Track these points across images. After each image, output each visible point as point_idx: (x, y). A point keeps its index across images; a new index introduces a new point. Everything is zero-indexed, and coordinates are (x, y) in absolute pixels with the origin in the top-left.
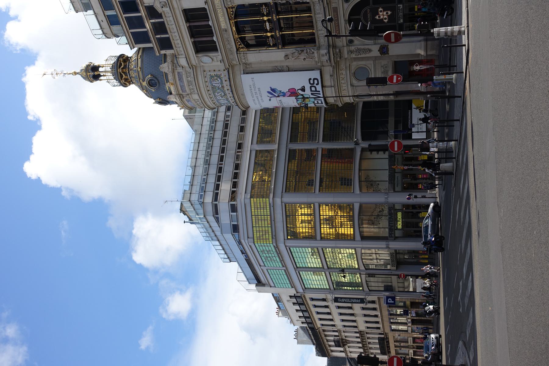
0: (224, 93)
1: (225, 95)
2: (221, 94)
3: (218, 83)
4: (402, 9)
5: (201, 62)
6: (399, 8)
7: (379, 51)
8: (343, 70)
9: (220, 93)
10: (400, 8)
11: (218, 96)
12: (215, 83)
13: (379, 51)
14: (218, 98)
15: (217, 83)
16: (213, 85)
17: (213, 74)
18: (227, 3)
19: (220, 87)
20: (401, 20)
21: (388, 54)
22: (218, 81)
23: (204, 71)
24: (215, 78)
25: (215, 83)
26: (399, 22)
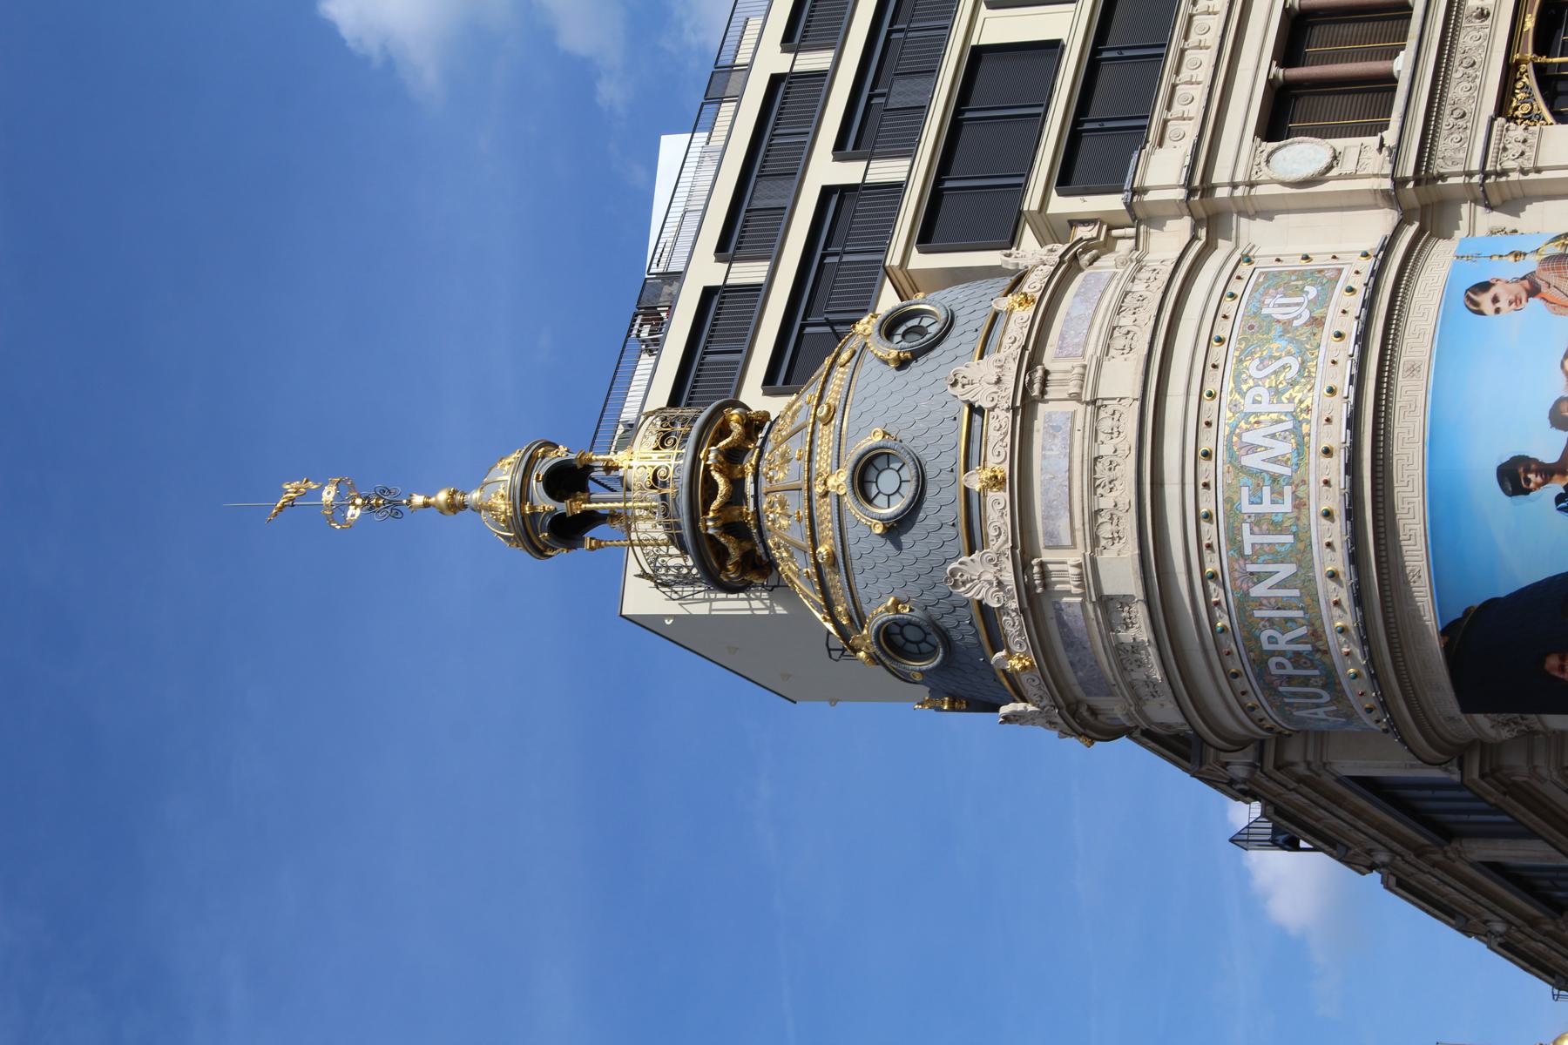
9: (1276, 365)
19: (1296, 323)
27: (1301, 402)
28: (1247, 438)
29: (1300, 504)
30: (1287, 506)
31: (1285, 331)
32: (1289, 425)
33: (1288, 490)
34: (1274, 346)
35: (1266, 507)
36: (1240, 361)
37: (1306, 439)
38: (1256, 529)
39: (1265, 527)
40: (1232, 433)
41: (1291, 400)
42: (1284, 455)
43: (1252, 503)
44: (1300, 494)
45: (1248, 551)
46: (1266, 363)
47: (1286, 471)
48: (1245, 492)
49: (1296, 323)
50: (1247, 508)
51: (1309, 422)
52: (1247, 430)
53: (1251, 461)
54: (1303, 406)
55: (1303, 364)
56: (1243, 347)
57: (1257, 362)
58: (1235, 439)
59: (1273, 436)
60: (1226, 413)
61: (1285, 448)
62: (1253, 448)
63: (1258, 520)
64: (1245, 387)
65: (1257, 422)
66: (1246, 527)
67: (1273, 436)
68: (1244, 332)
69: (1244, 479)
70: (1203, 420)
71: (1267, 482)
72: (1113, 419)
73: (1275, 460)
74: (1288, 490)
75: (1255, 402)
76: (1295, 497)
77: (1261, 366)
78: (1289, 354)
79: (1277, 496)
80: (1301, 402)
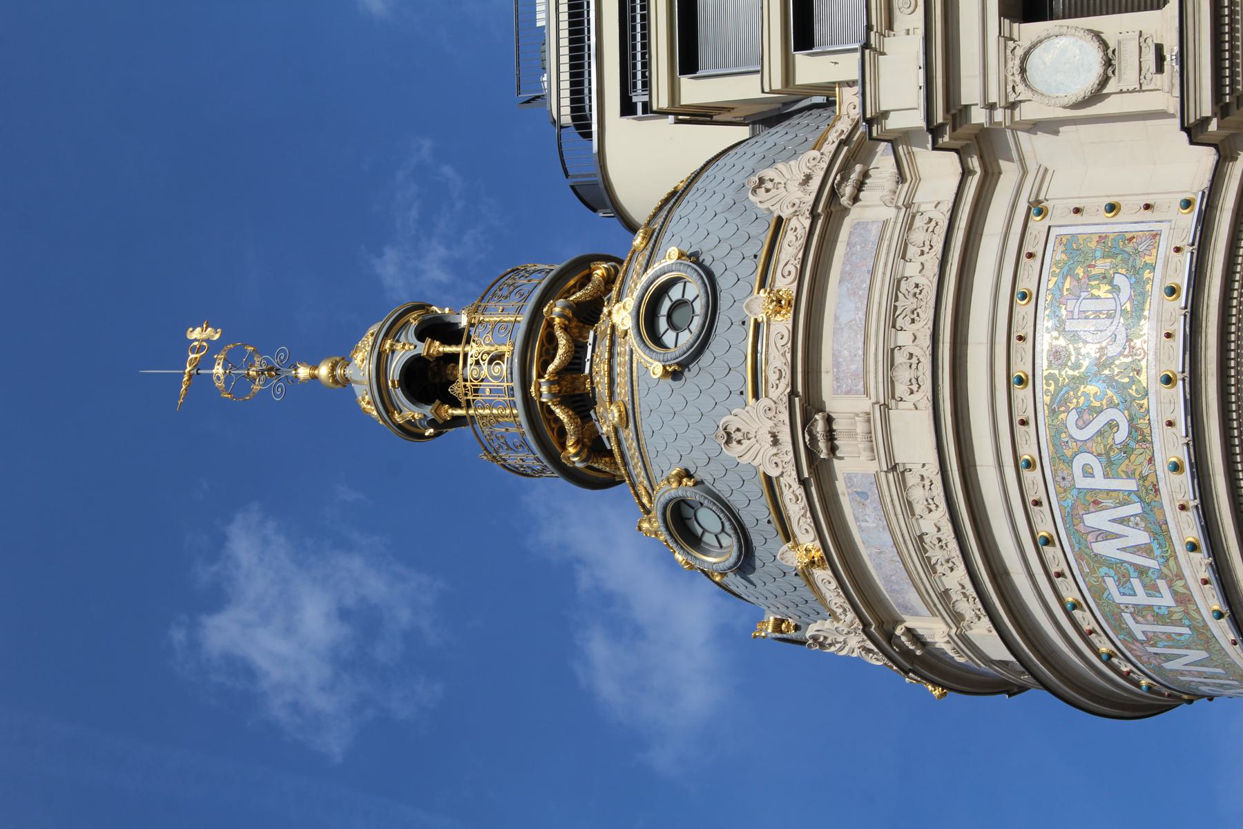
0: (1131, 420)
1: (1140, 436)
2: (1112, 425)
5: (1024, 80)
11: (1083, 447)
14: (1082, 483)
22: (1115, 289)
23: (1040, 212)
24: (1102, 266)
29: (1184, 599)
30: (1167, 600)
33: (1162, 584)
35: (1142, 598)
36: (1053, 412)
43: (1124, 594)
44: (1182, 590)
45: (1141, 637)
46: (1086, 417)
56: (1052, 388)
57: (1073, 416)
59: (1122, 521)
61: (1142, 537)
64: (1069, 453)
66: (1127, 617)
67: (1122, 521)
68: (1050, 366)
69: (1104, 570)
72: (924, 486)
73: (1137, 549)
74: (1162, 584)
76: (1175, 593)
77: (1080, 423)
78: (1112, 406)
79: (1152, 589)
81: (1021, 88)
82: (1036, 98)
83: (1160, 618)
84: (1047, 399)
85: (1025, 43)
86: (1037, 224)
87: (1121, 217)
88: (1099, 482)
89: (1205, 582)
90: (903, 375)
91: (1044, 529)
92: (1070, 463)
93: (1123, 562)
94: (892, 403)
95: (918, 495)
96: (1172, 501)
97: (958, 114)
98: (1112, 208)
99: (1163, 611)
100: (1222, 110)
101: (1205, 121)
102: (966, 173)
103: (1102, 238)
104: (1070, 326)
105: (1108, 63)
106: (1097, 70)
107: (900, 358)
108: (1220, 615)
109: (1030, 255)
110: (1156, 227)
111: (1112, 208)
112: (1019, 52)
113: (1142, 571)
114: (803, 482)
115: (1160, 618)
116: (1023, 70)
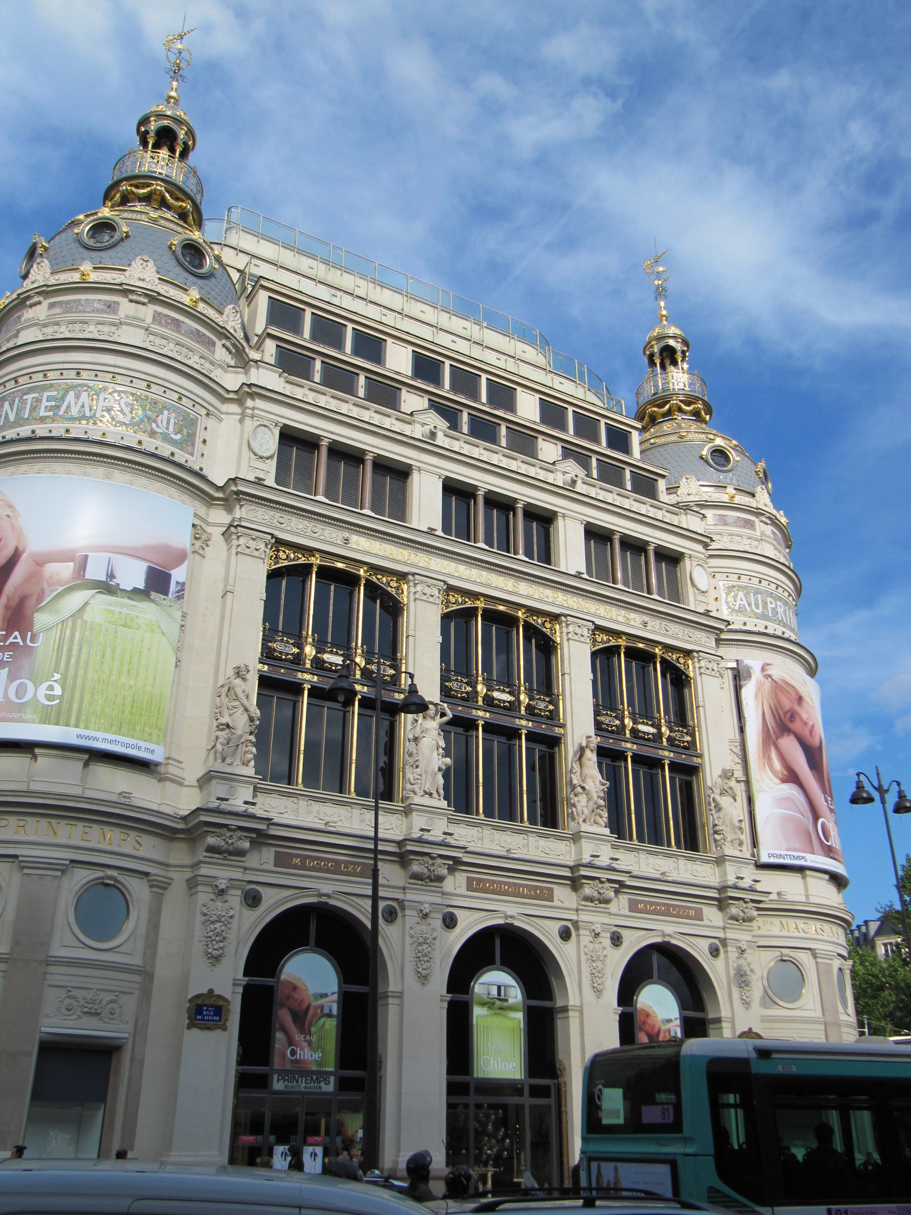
3: (167, 428)
4: (320, 1088)
6: (325, 1079)
7: (211, 991)
8: (137, 846)
9: (128, 413)
10: (322, 1084)
12: (169, 420)
13: (211, 991)
15: (168, 423)
16: (166, 412)
17: (200, 428)
18: (422, 582)
20: (281, 1082)
21: (189, 1028)
23: (208, 415)
25: (169, 420)
26: (275, 1076)
27: (101, 421)
28: (85, 394)
29: (42, 420)
30: (43, 413)
31: (149, 419)
32: (88, 414)
33: (51, 414)
34: (140, 412)
35: (45, 403)
36: (133, 395)
37: (77, 422)
38: (35, 400)
39: (35, 404)
40: (89, 387)
41: (103, 416)
42: (70, 411)
43: (48, 397)
44: (47, 420)
45: (25, 397)
47: (61, 413)
48: (55, 393)
49: (154, 425)
50: (46, 394)
51: (87, 424)
52: (89, 394)
53: (71, 396)
54: (98, 422)
55: (124, 423)
57: (131, 402)
58: (85, 388)
59: (83, 406)
60: (101, 385)
61: (74, 412)
62: (77, 397)
63: (38, 401)
64: (116, 395)
65: (92, 400)
66: (36, 395)
67: (83, 406)
68: (152, 399)
69: (61, 393)
70: (99, 373)
71: (57, 404)
73: (69, 407)
74: (51, 414)
75: (105, 399)
76: (46, 417)
78: (133, 418)
79: (50, 409)
80: (101, 421)
81: (258, 423)
82: (254, 428)
83: (34, 409)
84: (139, 394)
85: (274, 430)
86: (204, 412)
87: (201, 445)
88: (101, 403)
89: (50, 431)
90: (158, 341)
91: (84, 374)
92: (111, 394)
93: (64, 401)
94: (147, 332)
95: (106, 329)
96: (90, 429)
97: (252, 396)
98: (205, 441)
99: (37, 410)
100: (238, 493)
101: (236, 486)
102: (228, 391)
103: (195, 434)
104: (166, 412)
105: (261, 457)
106: (260, 454)
107: (164, 342)
108: (33, 432)
109: (194, 405)
110: (195, 455)
111: (205, 441)
112: (271, 427)
113: (58, 407)
114: (121, 285)
115: (34, 409)
116: (265, 426)
